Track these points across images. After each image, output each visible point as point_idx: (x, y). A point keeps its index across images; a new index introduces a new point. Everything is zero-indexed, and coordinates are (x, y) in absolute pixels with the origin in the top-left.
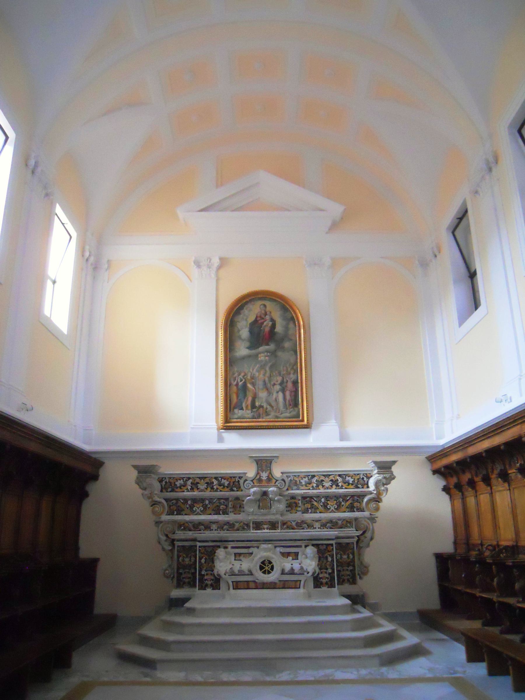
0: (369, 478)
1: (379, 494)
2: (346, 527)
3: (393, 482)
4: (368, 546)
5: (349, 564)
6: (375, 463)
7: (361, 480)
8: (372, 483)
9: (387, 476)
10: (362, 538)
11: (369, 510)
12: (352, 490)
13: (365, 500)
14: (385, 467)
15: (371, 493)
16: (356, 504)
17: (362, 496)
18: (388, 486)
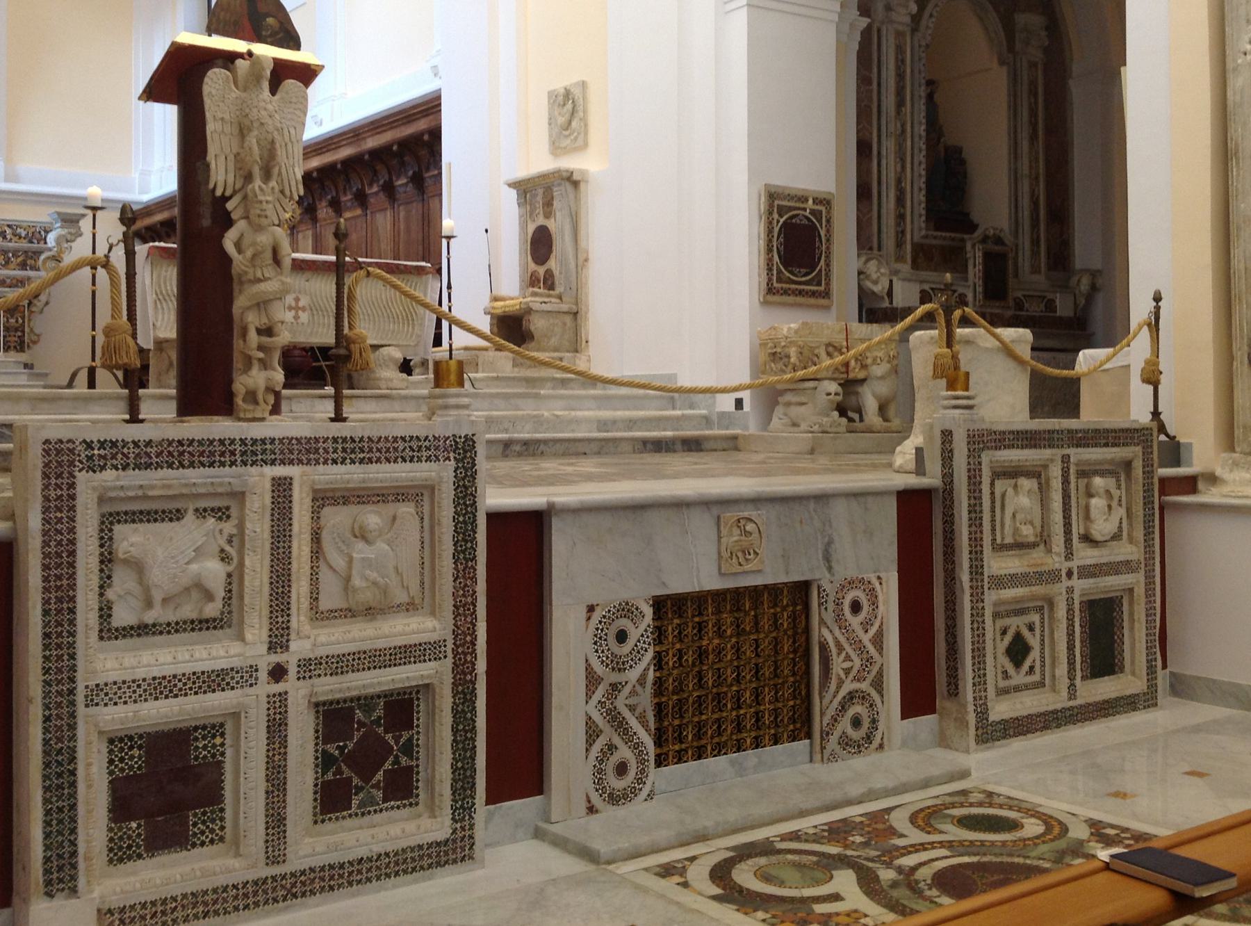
0: (47, 232)
1: (60, 252)
2: (16, 286)
3: (79, 240)
4: (41, 312)
5: (16, 330)
6: (59, 214)
7: (37, 235)
8: (51, 238)
9: (72, 231)
10: (35, 302)
11: (46, 270)
12: (24, 244)
13: (42, 257)
14: (71, 221)
15: (50, 250)
16: (29, 262)
17: (38, 253)
18: (73, 244)
